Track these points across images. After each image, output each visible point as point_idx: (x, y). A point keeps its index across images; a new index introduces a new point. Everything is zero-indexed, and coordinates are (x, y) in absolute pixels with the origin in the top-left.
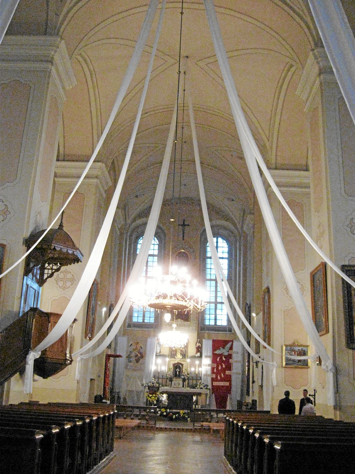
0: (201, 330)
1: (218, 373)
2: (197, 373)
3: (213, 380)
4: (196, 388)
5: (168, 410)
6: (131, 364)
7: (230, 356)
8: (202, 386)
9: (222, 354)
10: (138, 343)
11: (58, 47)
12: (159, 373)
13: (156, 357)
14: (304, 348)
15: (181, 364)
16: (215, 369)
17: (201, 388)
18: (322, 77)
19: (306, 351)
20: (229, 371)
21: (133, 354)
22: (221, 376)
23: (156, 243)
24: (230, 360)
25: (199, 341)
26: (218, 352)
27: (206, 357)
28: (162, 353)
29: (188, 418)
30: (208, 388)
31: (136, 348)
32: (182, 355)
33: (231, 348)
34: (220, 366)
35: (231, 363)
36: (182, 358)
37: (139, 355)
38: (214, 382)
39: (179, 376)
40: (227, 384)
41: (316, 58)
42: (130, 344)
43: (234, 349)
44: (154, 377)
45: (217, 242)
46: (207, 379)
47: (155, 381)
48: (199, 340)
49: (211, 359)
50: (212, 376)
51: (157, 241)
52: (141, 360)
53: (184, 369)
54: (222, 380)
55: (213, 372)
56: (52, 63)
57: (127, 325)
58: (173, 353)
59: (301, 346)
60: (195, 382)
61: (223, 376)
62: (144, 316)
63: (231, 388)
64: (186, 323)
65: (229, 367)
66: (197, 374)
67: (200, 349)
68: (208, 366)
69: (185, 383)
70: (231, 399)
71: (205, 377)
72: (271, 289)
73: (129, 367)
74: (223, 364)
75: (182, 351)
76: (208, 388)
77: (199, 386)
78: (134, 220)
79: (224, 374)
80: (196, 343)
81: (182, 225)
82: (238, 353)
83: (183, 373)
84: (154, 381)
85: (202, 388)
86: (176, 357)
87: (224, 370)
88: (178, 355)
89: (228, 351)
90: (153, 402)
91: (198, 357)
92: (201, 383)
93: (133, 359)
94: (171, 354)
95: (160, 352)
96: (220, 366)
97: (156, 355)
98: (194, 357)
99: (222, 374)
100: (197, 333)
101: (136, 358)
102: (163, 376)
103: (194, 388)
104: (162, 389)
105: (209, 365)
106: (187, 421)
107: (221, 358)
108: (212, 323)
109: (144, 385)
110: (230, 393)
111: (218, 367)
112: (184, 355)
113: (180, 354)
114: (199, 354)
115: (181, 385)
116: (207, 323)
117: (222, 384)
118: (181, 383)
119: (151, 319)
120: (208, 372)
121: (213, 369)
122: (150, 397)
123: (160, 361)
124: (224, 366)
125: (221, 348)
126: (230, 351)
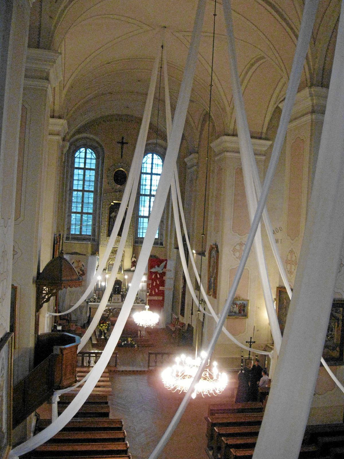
7: (163, 274)
8: (139, 302)
10: (80, 261)
11: (55, 62)
14: (245, 302)
18: (313, 116)
19: (246, 304)
20: (162, 287)
23: (93, 157)
24: (164, 277)
25: (135, 256)
26: (153, 270)
29: (135, 344)
33: (165, 267)
34: (155, 283)
35: (164, 280)
37: (81, 273)
39: (119, 293)
40: (161, 298)
41: (311, 95)
43: (168, 267)
45: (153, 159)
46: (143, 295)
48: (134, 255)
49: (147, 276)
51: (94, 155)
54: (156, 294)
56: (47, 79)
59: (243, 300)
61: (157, 291)
63: (163, 303)
65: (163, 283)
68: (144, 282)
72: (219, 247)
74: (158, 281)
76: (144, 302)
78: (74, 135)
79: (158, 289)
80: (132, 258)
81: (120, 143)
84: (95, 296)
85: (138, 303)
87: (157, 286)
89: (162, 270)
92: (138, 298)
96: (155, 283)
99: (156, 289)
105: (145, 282)
106: (134, 347)
109: (87, 300)
120: (144, 287)
121: (148, 285)
122: (101, 327)
124: (158, 283)
125: (156, 266)
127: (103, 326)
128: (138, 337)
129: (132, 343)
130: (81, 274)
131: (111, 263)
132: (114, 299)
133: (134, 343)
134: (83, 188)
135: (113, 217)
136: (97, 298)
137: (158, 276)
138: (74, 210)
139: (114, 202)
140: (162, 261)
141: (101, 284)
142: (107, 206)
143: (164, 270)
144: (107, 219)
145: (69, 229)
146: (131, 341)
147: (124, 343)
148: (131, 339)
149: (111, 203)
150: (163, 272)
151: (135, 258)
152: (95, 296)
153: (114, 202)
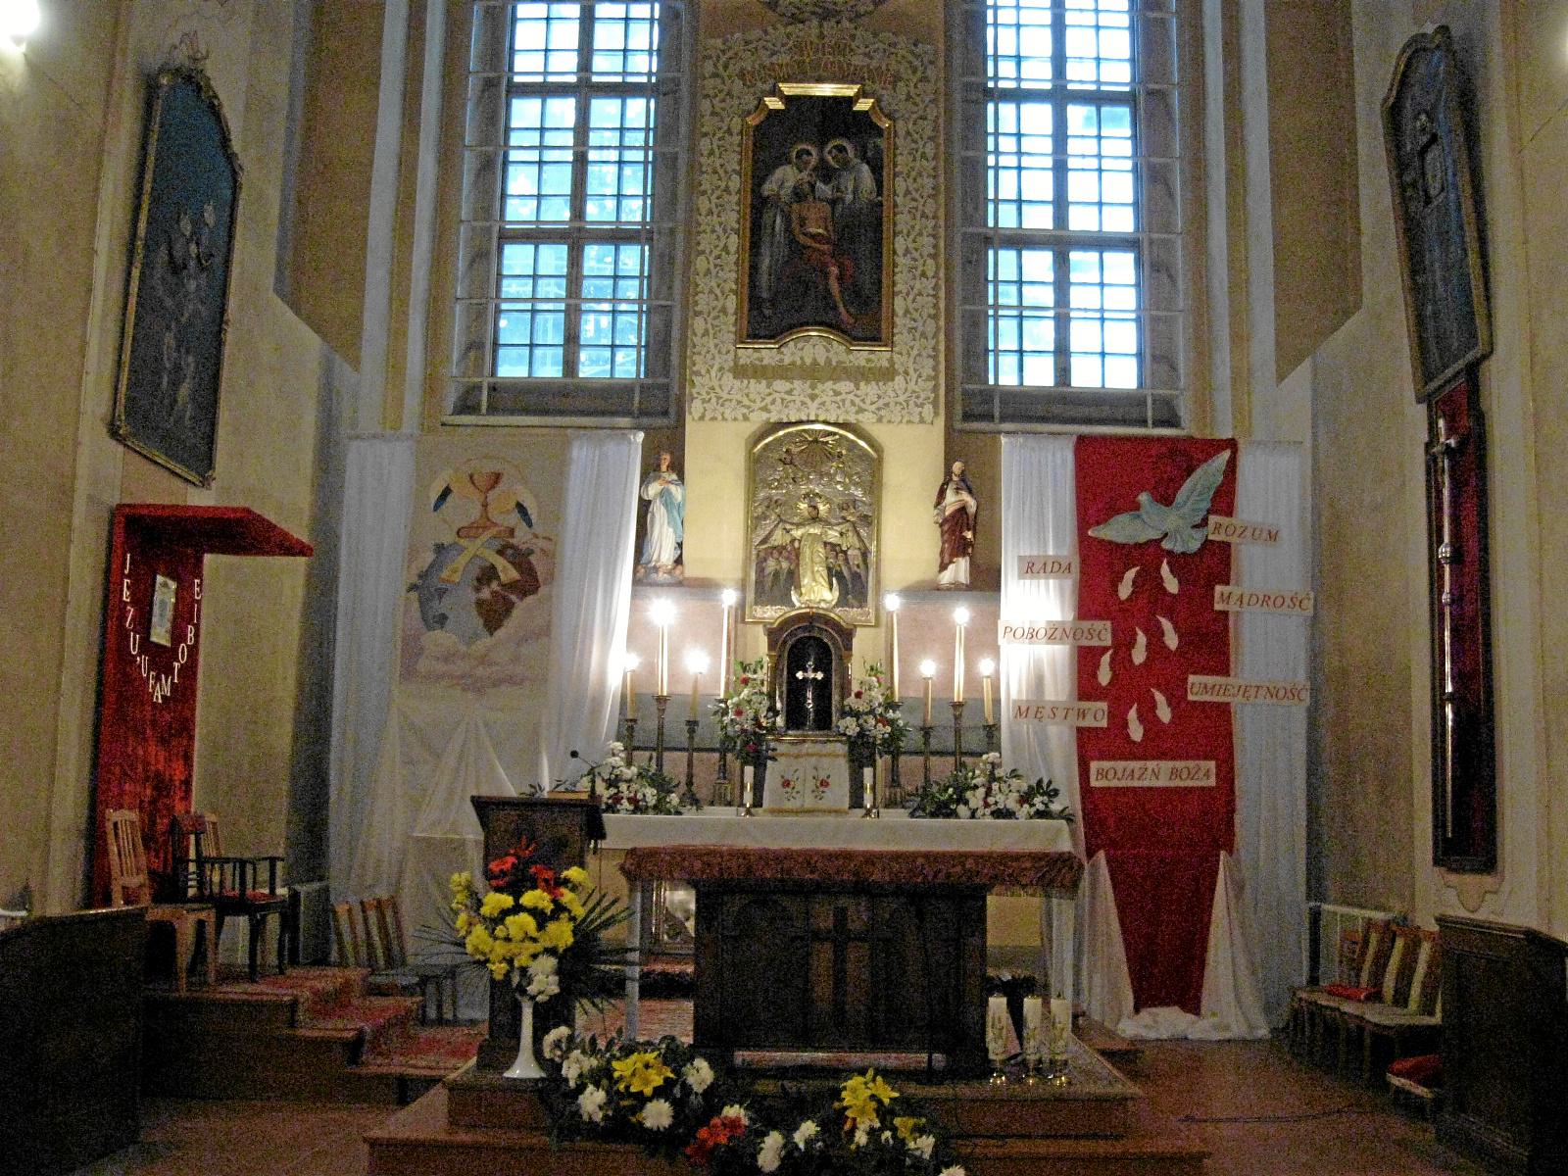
0: (967, 417)
1: (1128, 689)
2: (959, 693)
3: (1090, 745)
4: (962, 809)
5: (701, 1074)
6: (440, 639)
8: (1012, 804)
9: (1158, 542)
10: (497, 478)
12: (661, 700)
13: (634, 595)
15: (835, 625)
16: (1106, 659)
17: (999, 814)
20: (1210, 680)
21: (458, 569)
22: (1148, 716)
24: (1218, 589)
25: (963, 477)
26: (1119, 530)
27: (1031, 568)
28: (691, 570)
30: (1055, 807)
31: (485, 523)
32: (840, 577)
33: (1224, 499)
34: (1141, 639)
35: (1225, 614)
36: (837, 605)
37: (508, 573)
38: (1094, 765)
40: (1202, 774)
42: (434, 496)
44: (628, 730)
46: (1043, 742)
47: (629, 763)
48: (957, 467)
49: (1070, 583)
50: (1082, 714)
52: (522, 607)
53: (857, 671)
54: (1158, 745)
55: (1086, 687)
57: (451, 397)
58: (771, 565)
60: (942, 768)
61: (1164, 713)
62: (572, 340)
64: (861, 355)
66: (957, 706)
67: (969, 535)
68: (1051, 638)
69: (868, 772)
70: (1239, 887)
71: (1026, 726)
73: (423, 665)
74: (1167, 625)
75: (833, 547)
76: (1055, 807)
77: (981, 791)
80: (942, 494)
82: (1273, 536)
83: (851, 701)
84: (617, 761)
85: (1007, 814)
86: (794, 598)
87: (1168, 671)
88: (806, 581)
89: (1205, 522)
90: (524, 970)
91: (956, 588)
92: (999, 773)
93: (462, 605)
94: (760, 570)
95: (679, 561)
96: (1141, 639)
97: (637, 581)
98: (924, 592)
100: (940, 422)
101: (486, 594)
102: (692, 724)
103: (944, 810)
104: (623, 830)
105: (1054, 634)
107: (1149, 581)
108: (1040, 374)
110: (1230, 852)
111: (1123, 645)
112: (856, 576)
113: (822, 570)
114: (960, 570)
115: (839, 791)
116: (1008, 378)
117: (1158, 774)
118: (839, 770)
119: (620, 355)
121: (1086, 659)
123: (664, 610)
124: (1172, 641)
125: (1144, 498)
126: (1213, 519)
127: (517, 909)
128: (985, 1069)
129: (903, 1142)
130: (512, 586)
131: (779, 538)
132: (786, 784)
133: (925, 1145)
134: (585, 65)
135: (786, 193)
136: (630, 772)
137: (1172, 585)
138: (519, 212)
139: (789, 89)
140: (1186, 455)
141: (673, 663)
142: (736, 124)
143: (1218, 529)
144: (733, 216)
145: (483, 345)
146: (885, 1113)
147: (789, 1147)
148: (887, 1094)
149: (760, 101)
150: (1207, 544)
151: (970, 492)
152: (617, 761)
153: (789, 89)
